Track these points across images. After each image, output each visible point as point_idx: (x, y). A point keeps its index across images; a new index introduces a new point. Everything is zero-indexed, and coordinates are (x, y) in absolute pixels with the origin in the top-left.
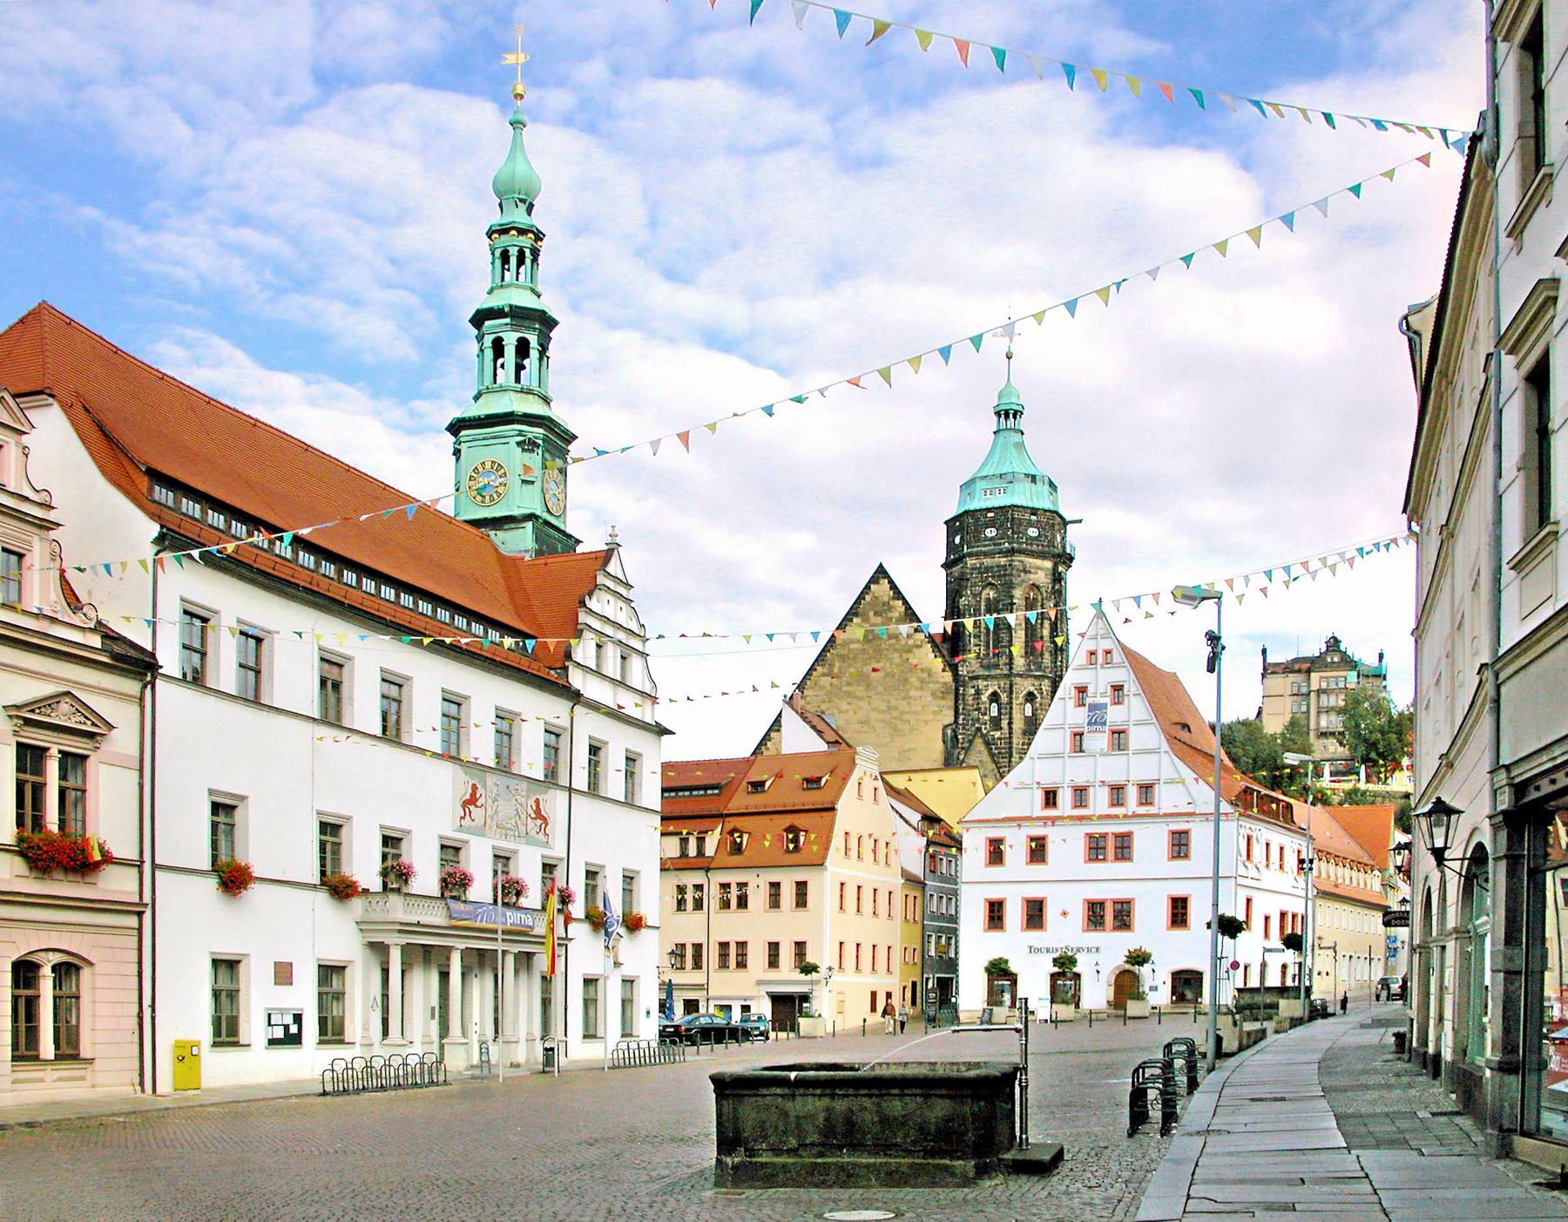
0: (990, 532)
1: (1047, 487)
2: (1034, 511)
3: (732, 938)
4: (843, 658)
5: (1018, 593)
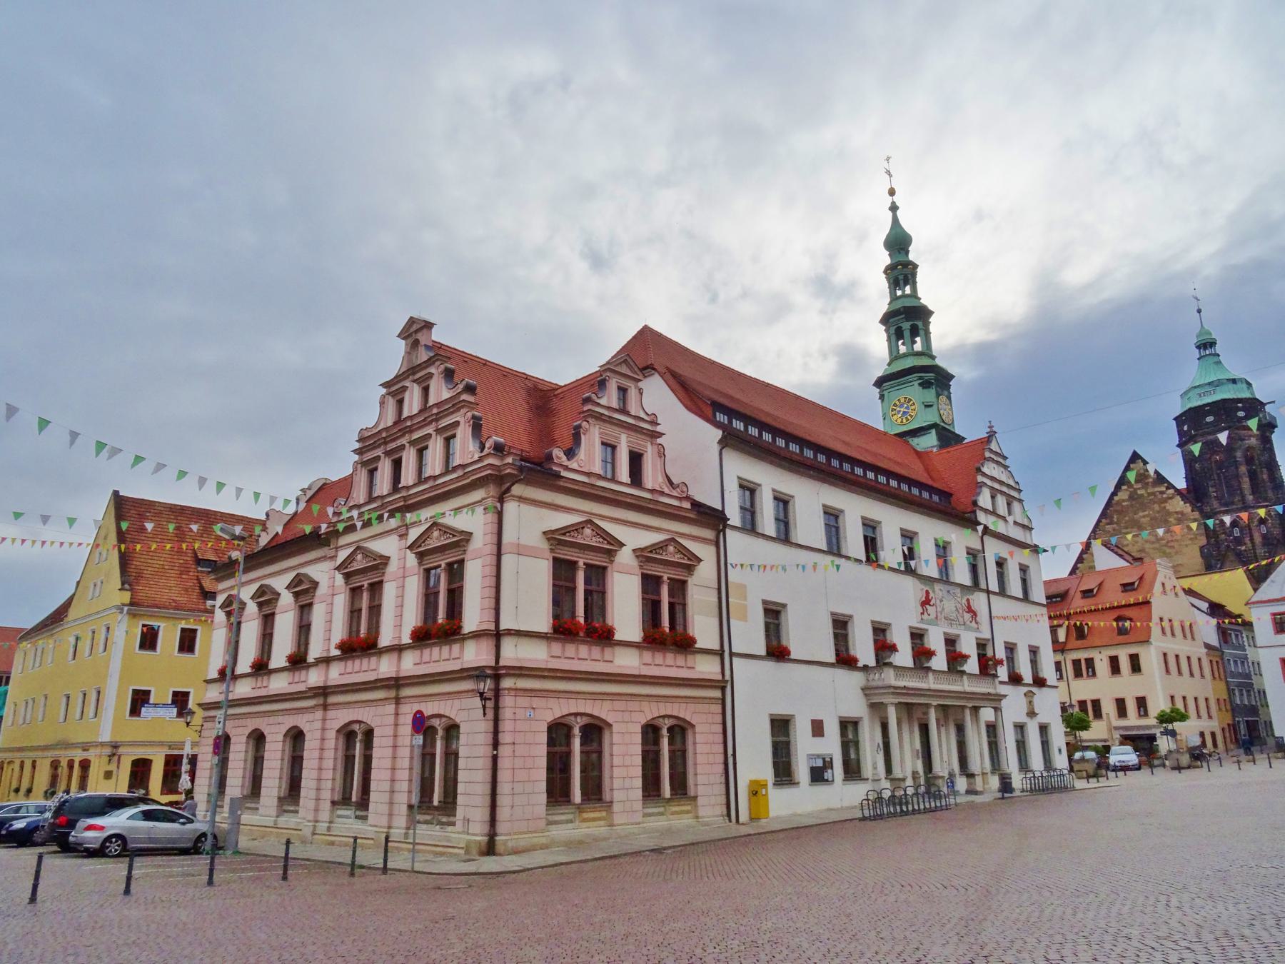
0: (1210, 419)
1: (1244, 386)
2: (1240, 400)
3: (1088, 696)
4: (1120, 512)
5: (1239, 454)
